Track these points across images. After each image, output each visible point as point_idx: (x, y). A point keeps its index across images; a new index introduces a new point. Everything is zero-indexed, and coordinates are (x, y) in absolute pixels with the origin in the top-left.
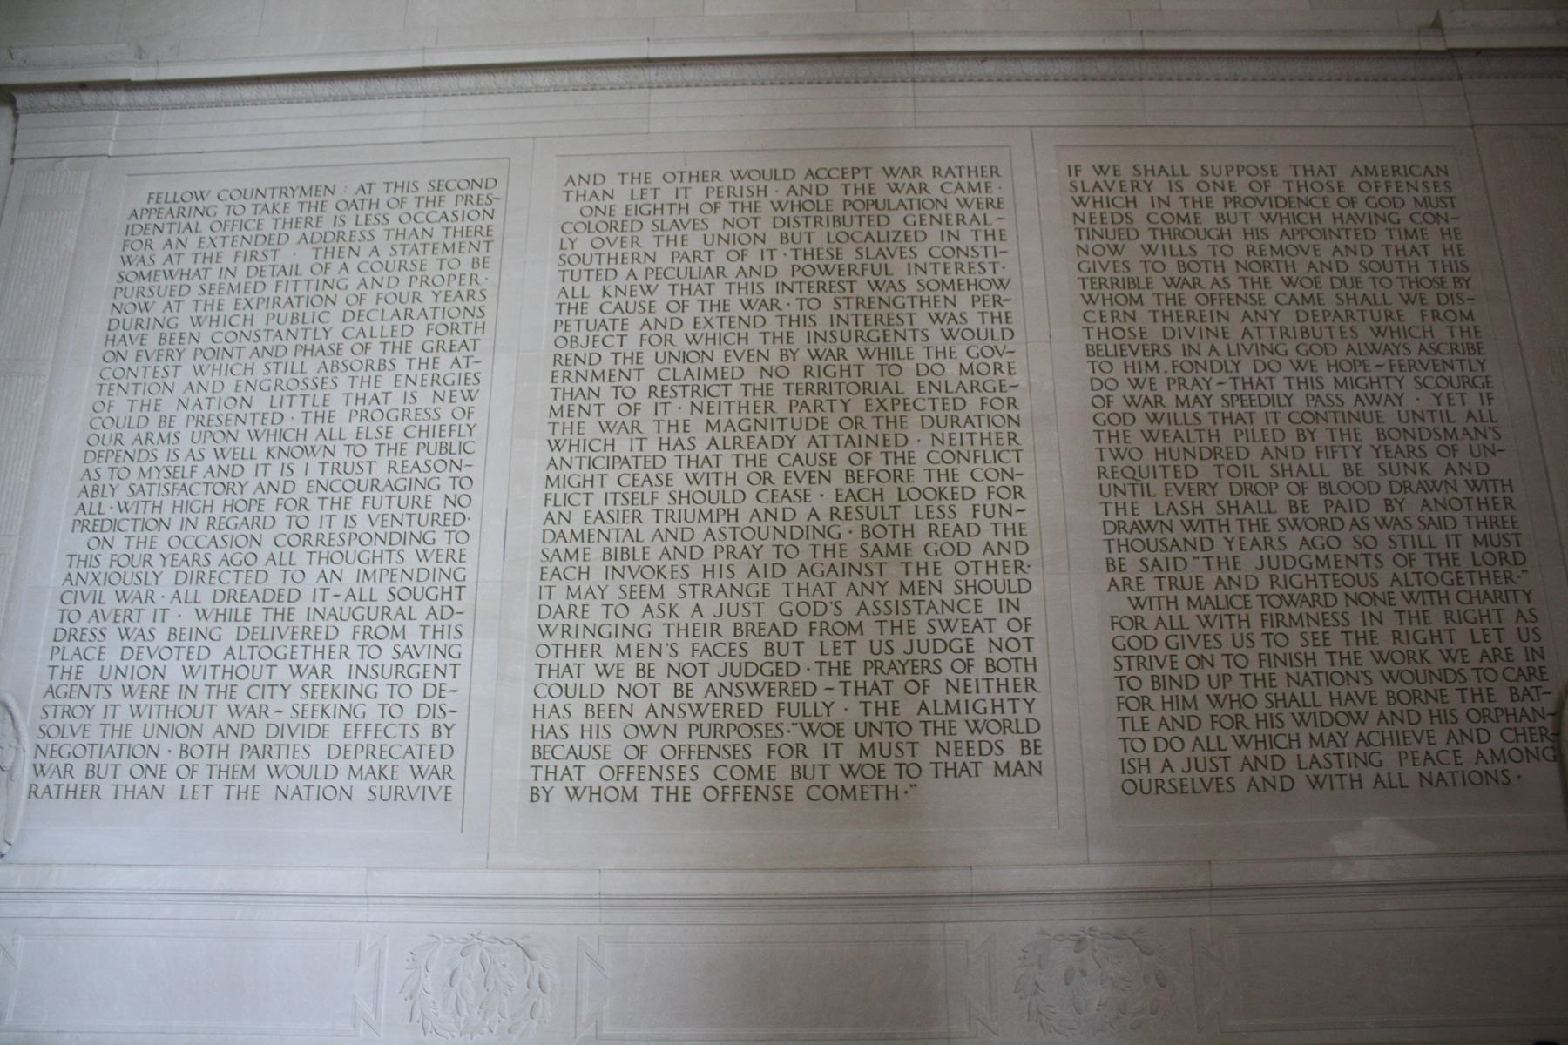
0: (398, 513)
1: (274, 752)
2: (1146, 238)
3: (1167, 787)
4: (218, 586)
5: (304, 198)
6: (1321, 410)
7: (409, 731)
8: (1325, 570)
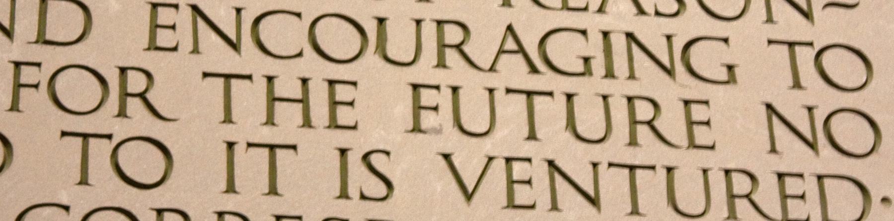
0: (576, 160)
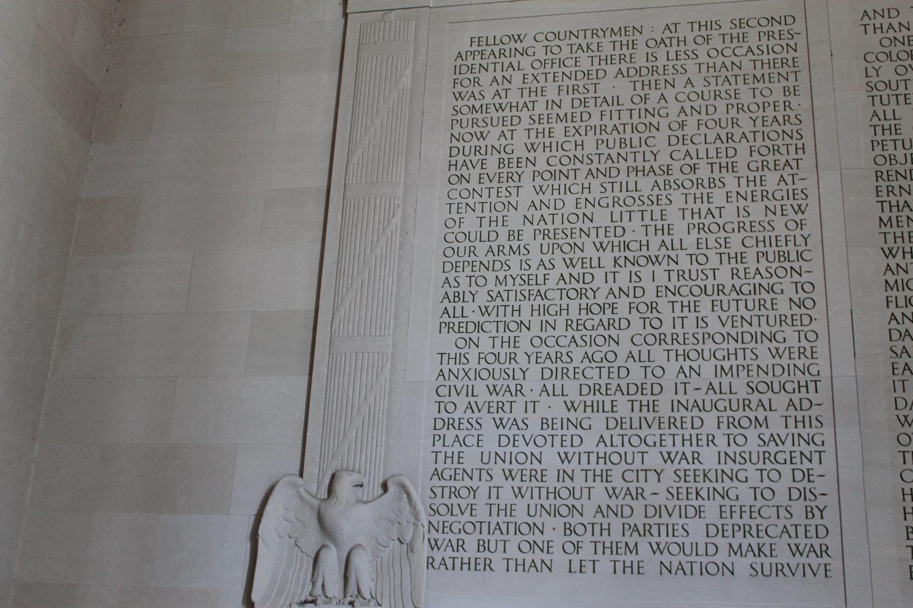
1: (654, 530)
4: (583, 381)
5: (614, 38)
7: (782, 512)
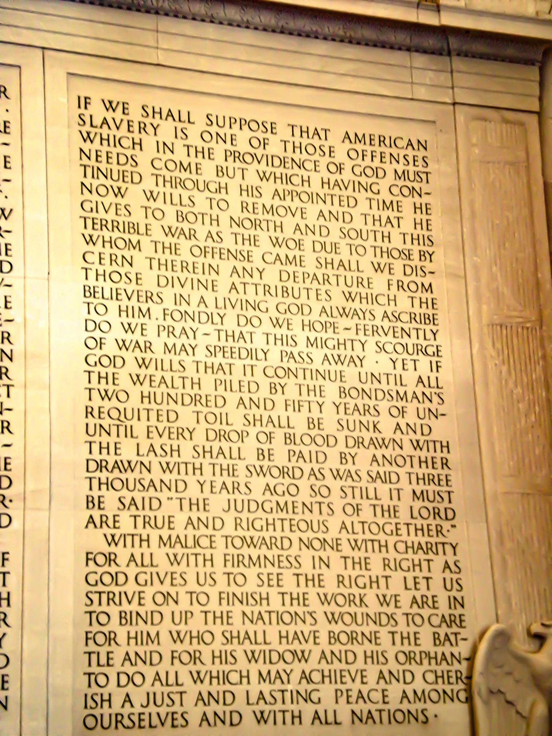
2: (149, 184)
3: (126, 722)
6: (292, 365)
8: (283, 515)
